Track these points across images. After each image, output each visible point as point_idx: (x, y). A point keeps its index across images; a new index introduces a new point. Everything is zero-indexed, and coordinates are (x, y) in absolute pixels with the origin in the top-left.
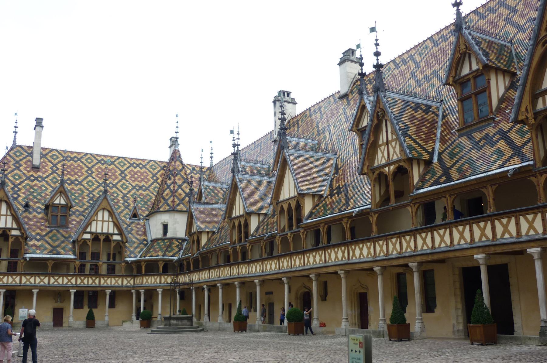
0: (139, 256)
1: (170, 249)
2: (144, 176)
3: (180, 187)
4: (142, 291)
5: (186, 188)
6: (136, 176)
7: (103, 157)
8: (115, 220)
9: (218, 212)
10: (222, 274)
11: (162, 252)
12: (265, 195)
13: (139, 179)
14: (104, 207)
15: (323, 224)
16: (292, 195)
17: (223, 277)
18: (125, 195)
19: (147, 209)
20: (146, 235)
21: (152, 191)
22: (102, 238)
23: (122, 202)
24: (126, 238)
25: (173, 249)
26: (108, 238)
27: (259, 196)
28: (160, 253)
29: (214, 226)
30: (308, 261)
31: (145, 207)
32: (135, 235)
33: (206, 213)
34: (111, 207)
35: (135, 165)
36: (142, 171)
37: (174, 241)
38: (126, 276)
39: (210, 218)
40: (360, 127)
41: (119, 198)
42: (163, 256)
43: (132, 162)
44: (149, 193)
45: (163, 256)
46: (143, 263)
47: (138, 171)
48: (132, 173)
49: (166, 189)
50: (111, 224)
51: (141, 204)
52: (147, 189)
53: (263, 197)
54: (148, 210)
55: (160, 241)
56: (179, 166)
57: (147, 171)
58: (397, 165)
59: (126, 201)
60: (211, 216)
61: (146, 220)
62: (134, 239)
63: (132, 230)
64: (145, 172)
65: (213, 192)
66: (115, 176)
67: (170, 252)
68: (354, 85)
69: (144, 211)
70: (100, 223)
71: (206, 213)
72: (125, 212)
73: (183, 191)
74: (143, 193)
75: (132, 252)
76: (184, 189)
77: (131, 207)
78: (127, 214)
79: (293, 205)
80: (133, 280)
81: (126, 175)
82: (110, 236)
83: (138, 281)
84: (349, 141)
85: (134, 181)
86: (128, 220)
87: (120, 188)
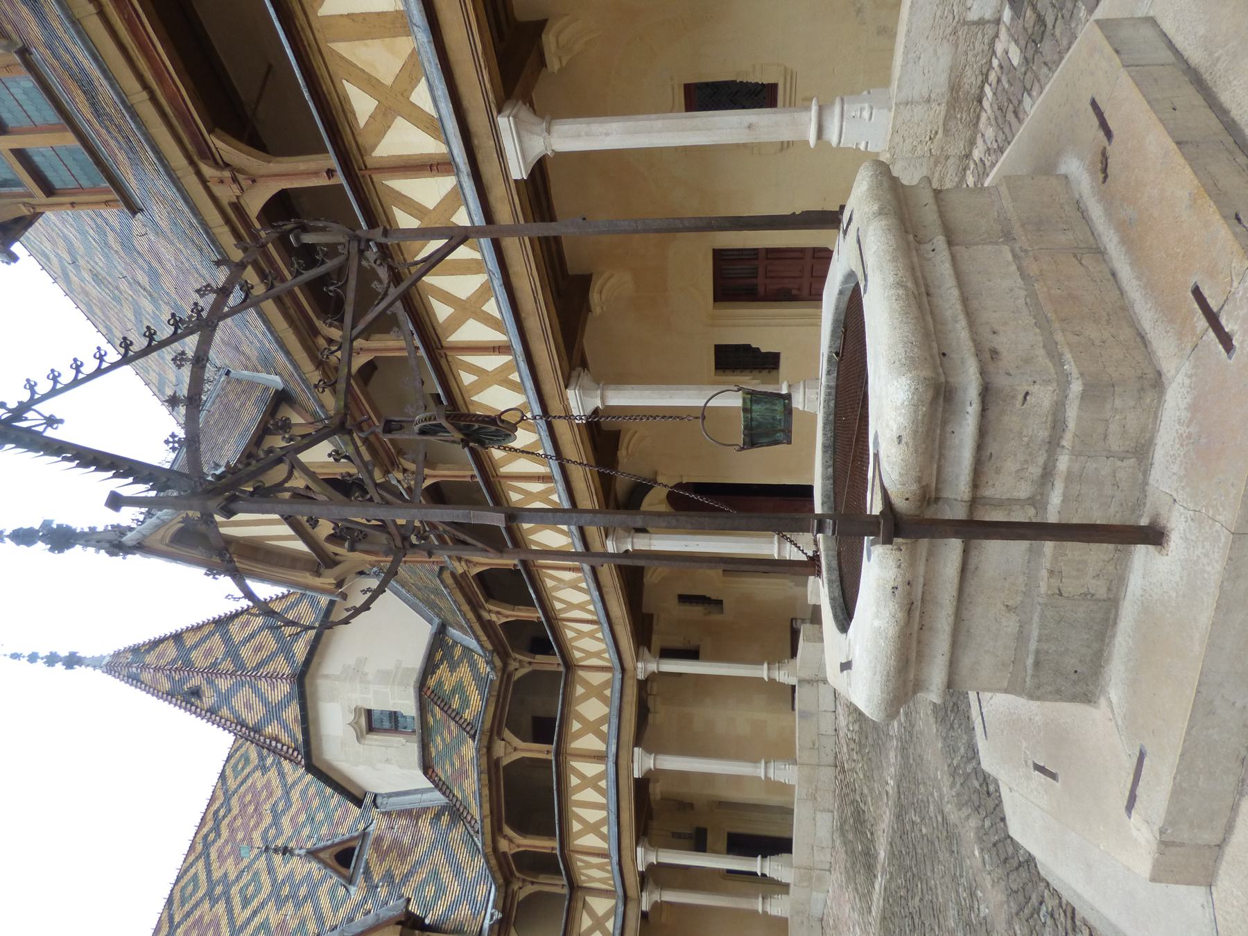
1: (455, 704)
4: (644, 857)
11: (462, 742)
20: (425, 810)
25: (459, 688)
37: (432, 682)
42: (473, 737)
43: (199, 847)
44: (300, 787)
46: (504, 845)
47: (230, 825)
49: (231, 709)
57: (243, 789)
67: (465, 702)
72: (325, 902)
78: (332, 893)
80: (589, 899)
83: (594, 873)
86: (353, 889)
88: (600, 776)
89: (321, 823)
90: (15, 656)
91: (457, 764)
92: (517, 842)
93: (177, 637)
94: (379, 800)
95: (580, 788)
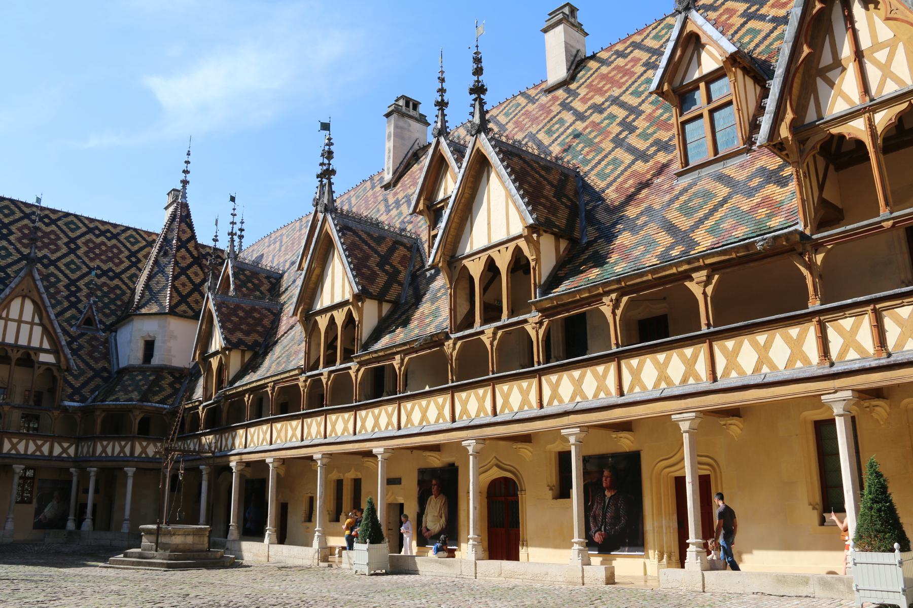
0: (90, 400)
2: (112, 252)
3: (184, 271)
5: (196, 274)
6: (97, 251)
7: (34, 209)
8: (46, 322)
9: (266, 317)
10: (279, 436)
11: (139, 392)
12: (392, 266)
13: (103, 257)
14: (26, 292)
15: (614, 296)
16: (499, 235)
17: (278, 444)
18: (73, 282)
19: (113, 312)
20: (109, 362)
21: (126, 280)
22: (15, 355)
23: (65, 293)
24: (67, 360)
25: (162, 389)
26: (27, 357)
27: (381, 265)
28: (135, 395)
29: (256, 341)
30: (555, 395)
31: (110, 309)
32: (87, 358)
33: (241, 314)
34: (40, 294)
35: (97, 232)
36: (109, 244)
38: (60, 439)
39: (248, 324)
40: (677, 83)
41: (61, 286)
42: (141, 400)
43: (91, 226)
44: (120, 283)
45: (141, 400)
46: (98, 413)
47: (103, 243)
48: (91, 245)
49: (156, 274)
50: (38, 330)
51: (103, 302)
52: (117, 276)
53: (387, 267)
54: (116, 315)
55: (135, 373)
56: (184, 232)
57: (119, 245)
59: (73, 294)
60: (250, 321)
61: (111, 332)
62: (82, 366)
63: (81, 347)
64: (114, 246)
65: (251, 282)
66: (56, 245)
67: (156, 393)
69: (107, 316)
70: (12, 326)
71: (241, 314)
72: (68, 314)
73: (188, 277)
74: (109, 282)
75: (77, 391)
76: (192, 276)
77: (80, 306)
78: (73, 317)
79: (503, 261)
80: (74, 446)
81: (78, 247)
82: (32, 353)
83: (85, 449)
84: (607, 145)
85: (92, 260)
87: (63, 268)
88: (124, 453)
89: (103, 302)
90: (189, 154)
91: (130, 388)
92: (99, 418)
93: (193, 237)
94: (114, 334)
95: (120, 445)
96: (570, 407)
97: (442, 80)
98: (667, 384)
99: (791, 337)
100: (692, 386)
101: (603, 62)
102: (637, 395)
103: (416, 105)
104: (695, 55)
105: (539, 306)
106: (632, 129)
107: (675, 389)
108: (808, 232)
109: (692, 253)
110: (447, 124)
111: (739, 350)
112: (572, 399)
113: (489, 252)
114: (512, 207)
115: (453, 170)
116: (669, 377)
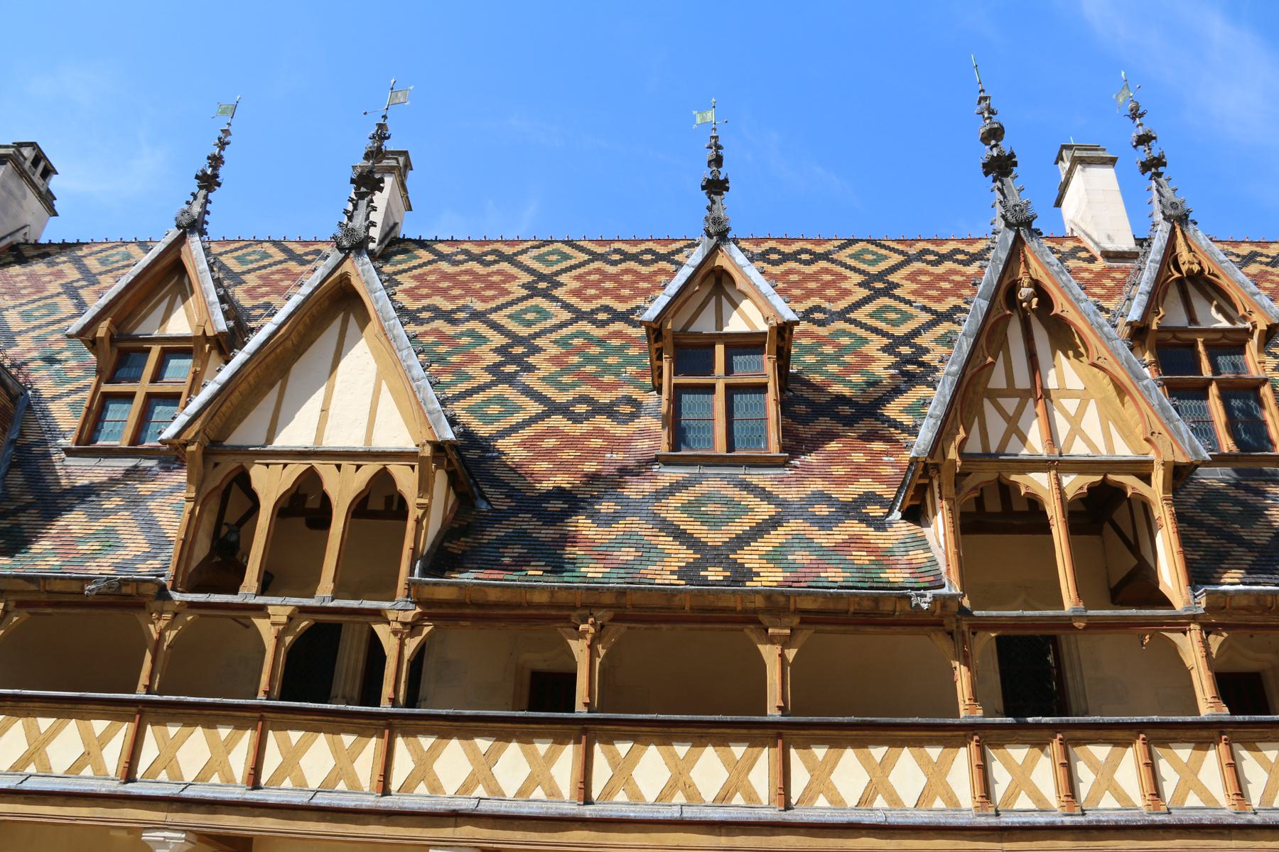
30: (423, 771)
58: (1099, 478)
68: (389, 245)
79: (343, 487)
96: (465, 804)
97: (223, 144)
98: (688, 797)
99: (930, 759)
100: (737, 809)
101: (442, 257)
102: (615, 807)
103: (48, 172)
104: (713, 301)
105: (427, 593)
106: (530, 368)
107: (708, 810)
108: (966, 603)
109: (748, 584)
110: (207, 218)
111: (836, 763)
112: (465, 789)
113: (315, 463)
114: (387, 402)
115: (204, 294)
116: (692, 785)
